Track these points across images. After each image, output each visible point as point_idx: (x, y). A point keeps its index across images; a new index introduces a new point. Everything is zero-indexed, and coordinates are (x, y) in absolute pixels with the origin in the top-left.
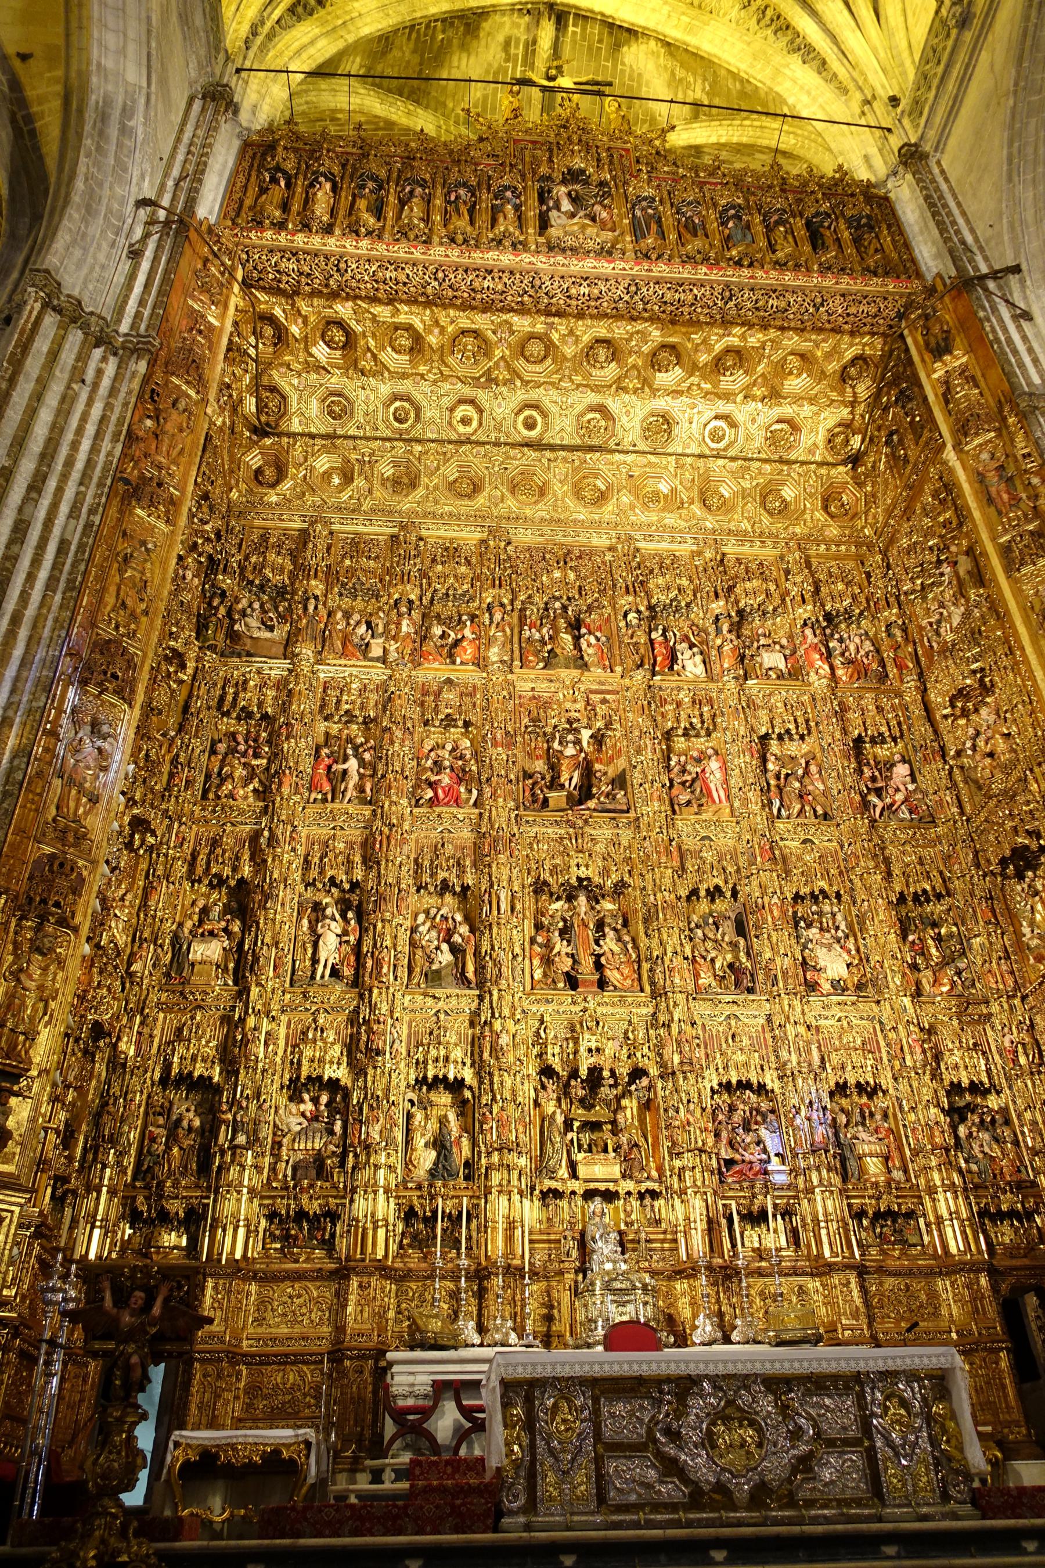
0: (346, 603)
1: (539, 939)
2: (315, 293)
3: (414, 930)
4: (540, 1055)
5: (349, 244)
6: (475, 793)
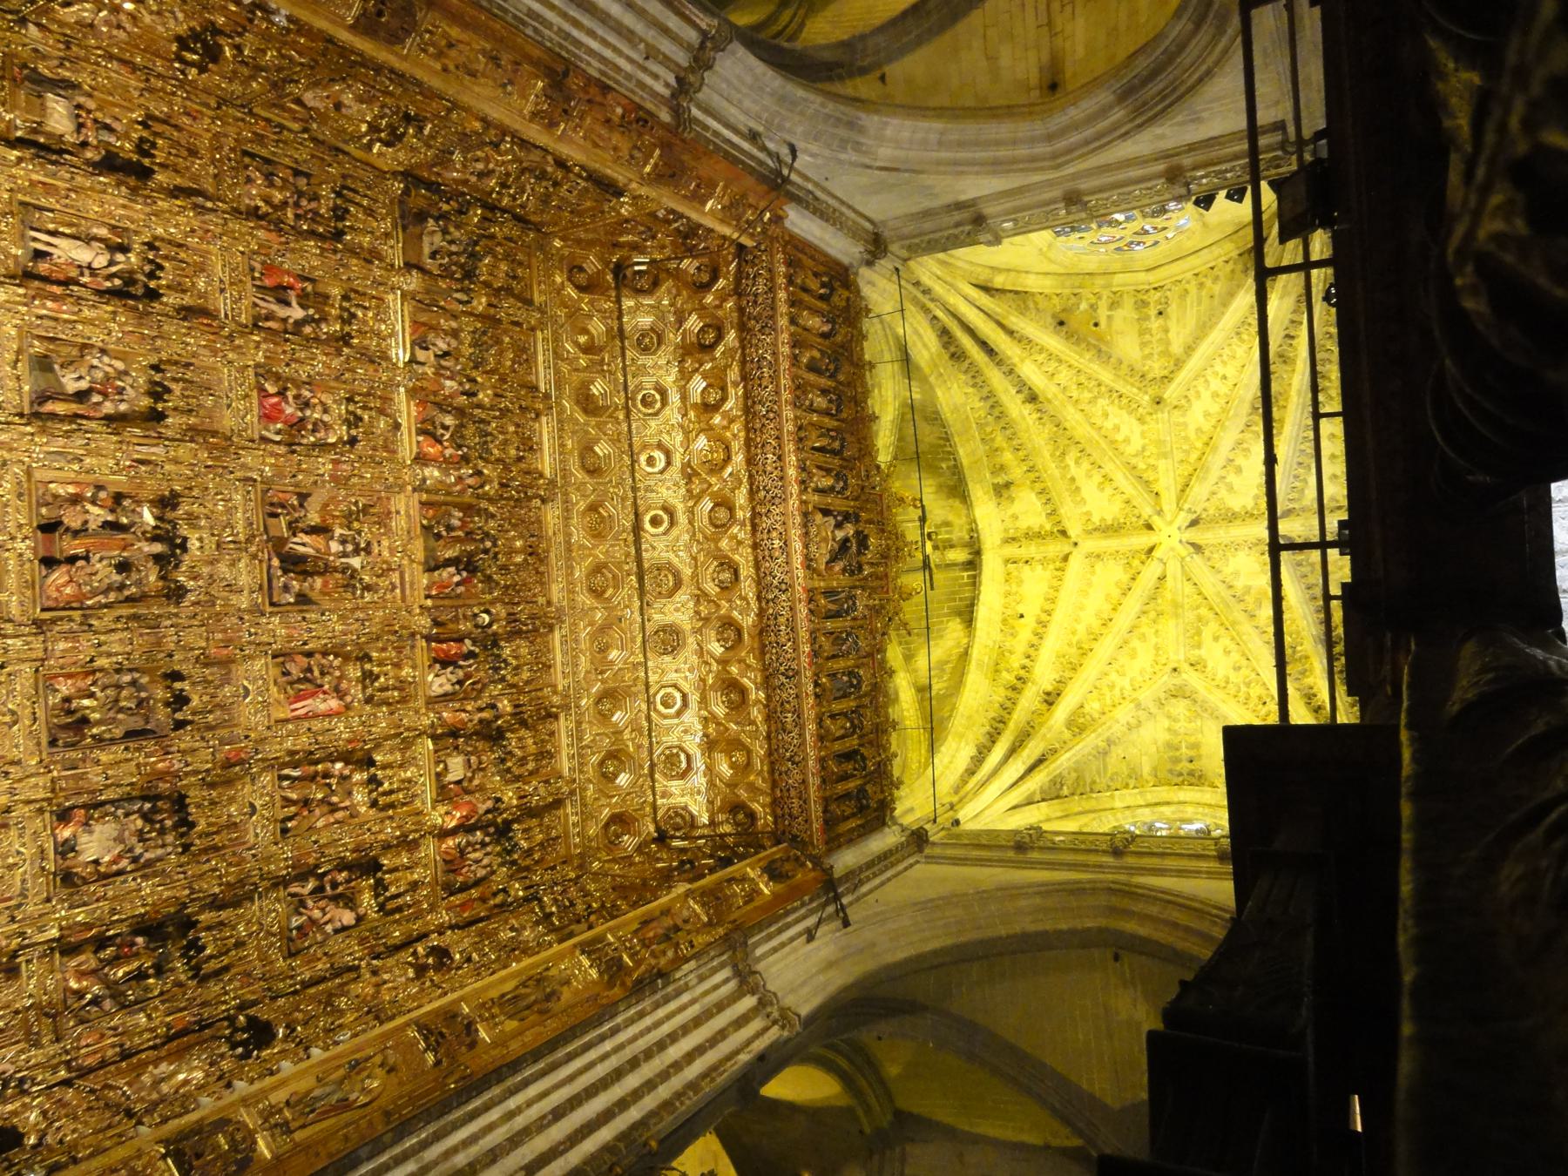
2: (741, 310)
5: (785, 337)
6: (278, 438)
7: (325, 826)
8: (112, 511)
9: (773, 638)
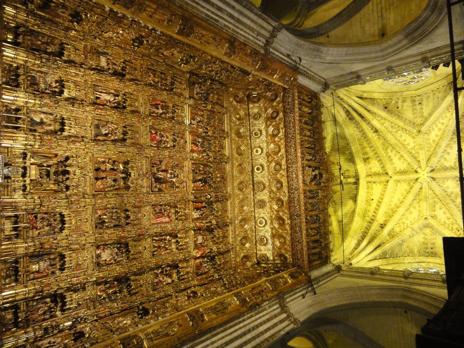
0: (205, 117)
2: (284, 107)
4: (73, 157)
5: (297, 114)
6: (155, 145)
7: (164, 254)
8: (113, 165)
9: (293, 204)
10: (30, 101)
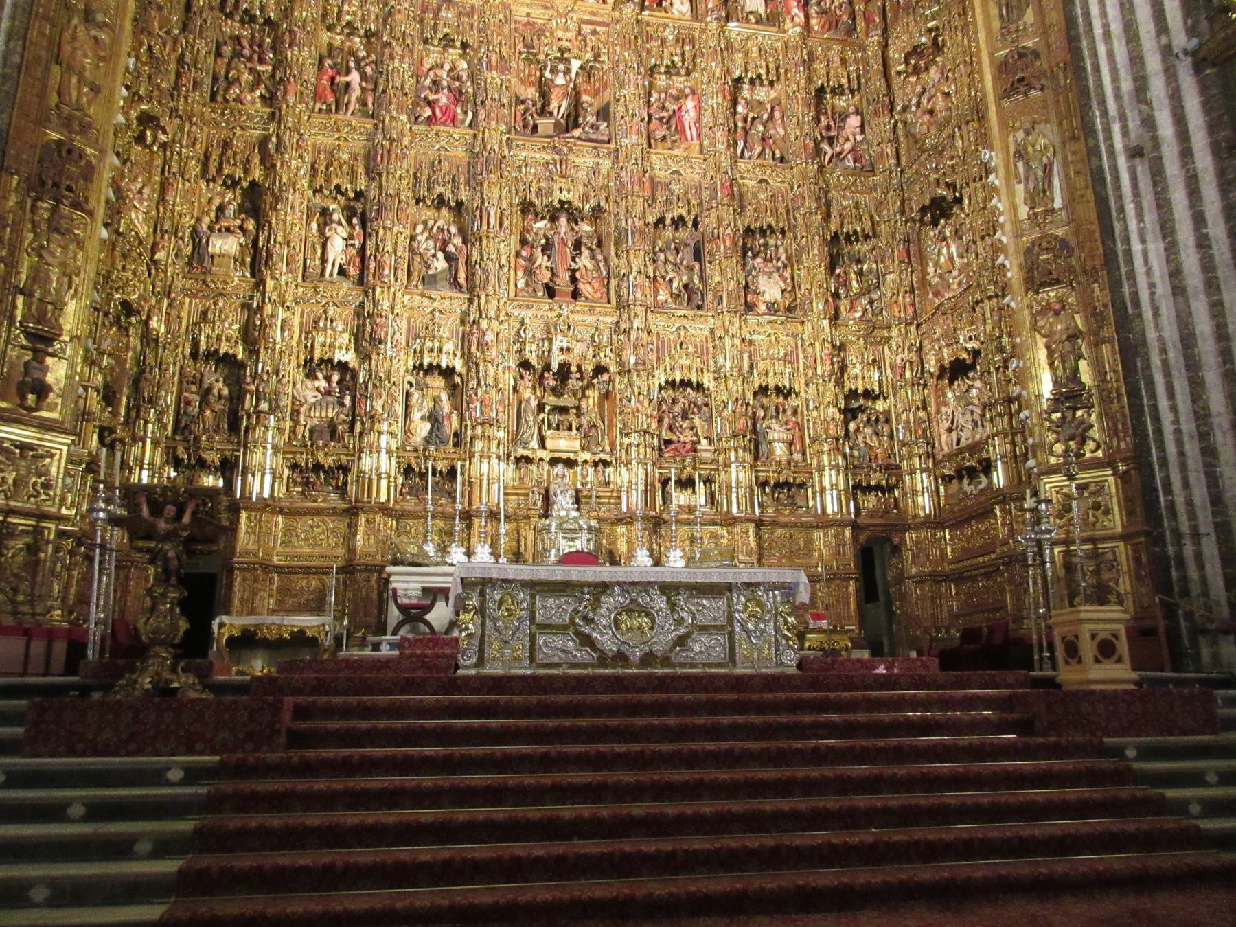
1: (524, 253)
3: (413, 238)
4: (520, 351)
6: (470, 114)
10: (384, 445)
